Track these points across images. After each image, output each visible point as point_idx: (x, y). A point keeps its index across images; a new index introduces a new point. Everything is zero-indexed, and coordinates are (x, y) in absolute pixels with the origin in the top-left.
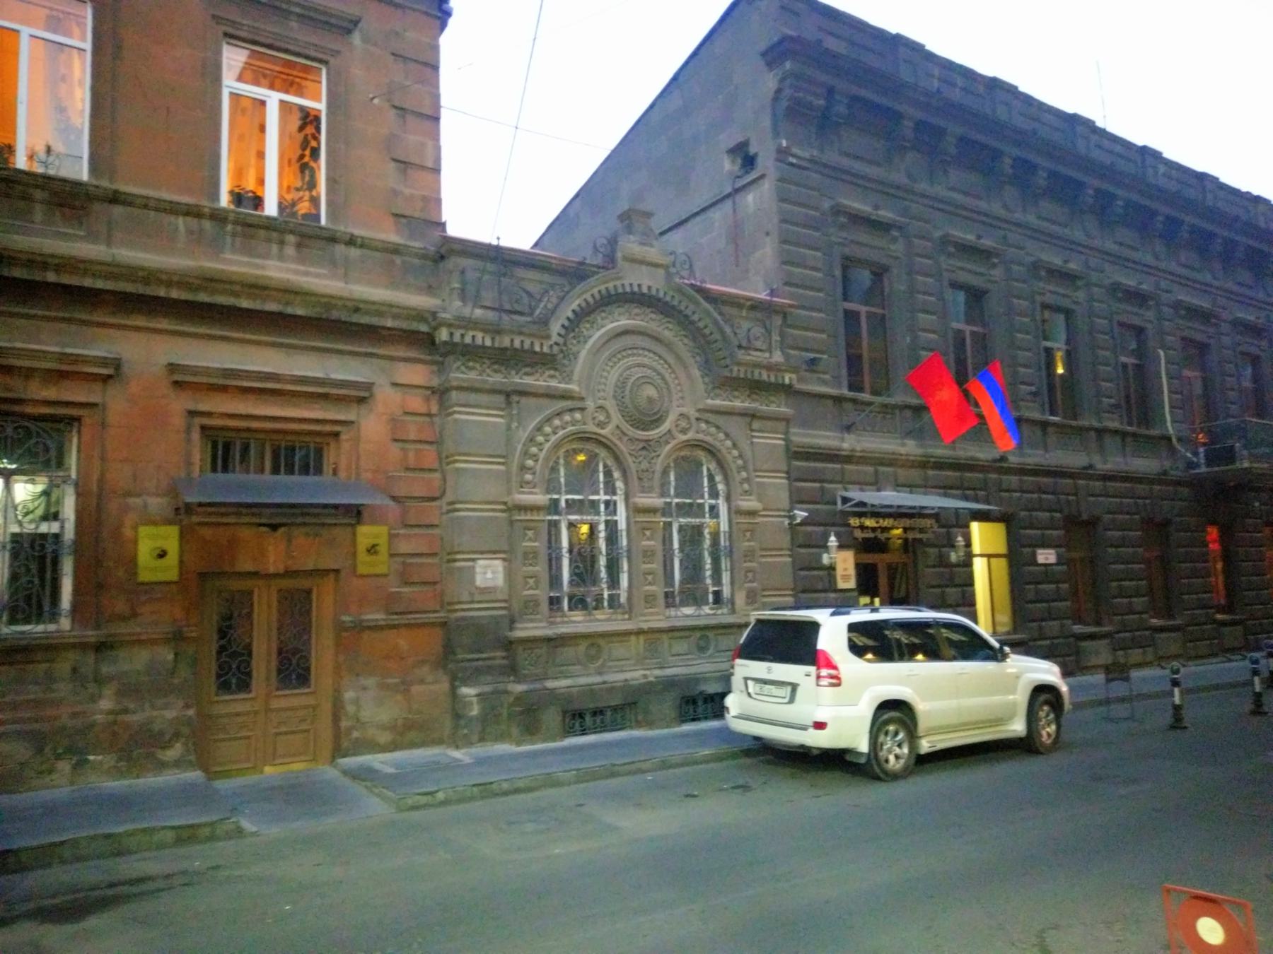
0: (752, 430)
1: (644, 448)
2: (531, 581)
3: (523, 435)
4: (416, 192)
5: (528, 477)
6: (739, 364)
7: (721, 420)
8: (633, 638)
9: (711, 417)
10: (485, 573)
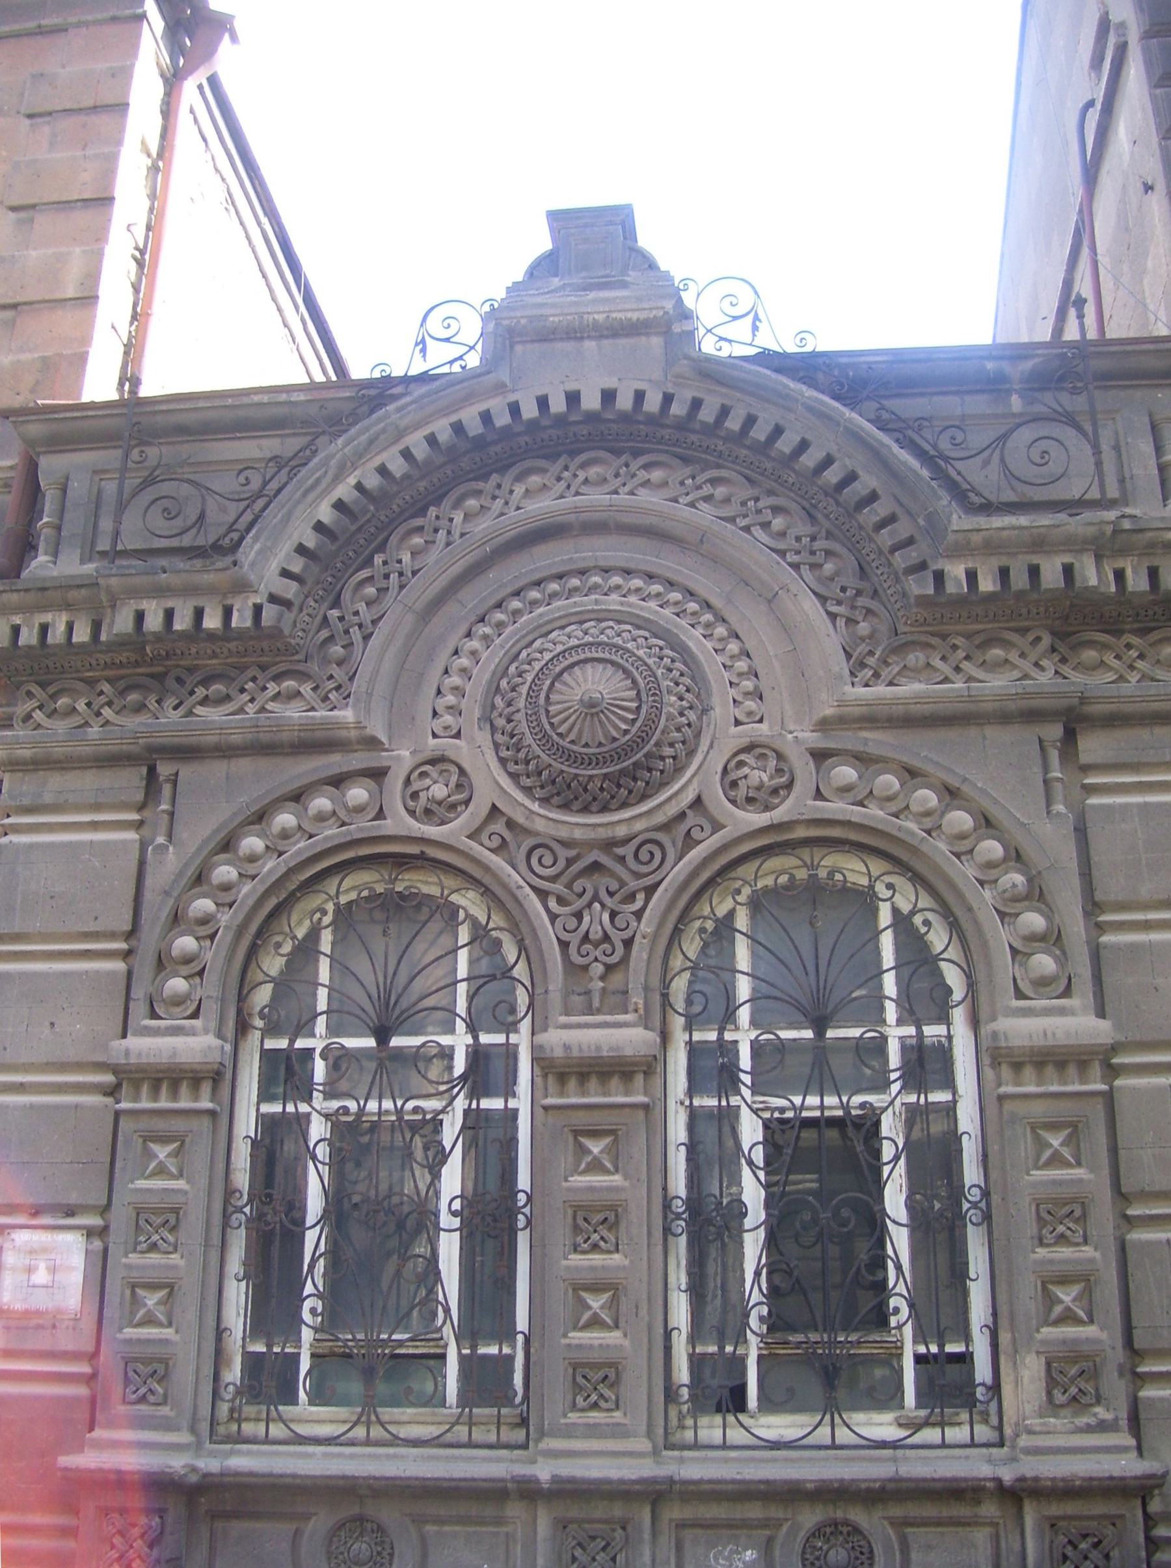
0: (1086, 769)
1: (596, 867)
2: (152, 1300)
3: (168, 866)
4: (26, 357)
5: (177, 985)
6: (959, 551)
7: (919, 747)
8: (515, 1510)
9: (875, 740)
10: (30, 1270)
